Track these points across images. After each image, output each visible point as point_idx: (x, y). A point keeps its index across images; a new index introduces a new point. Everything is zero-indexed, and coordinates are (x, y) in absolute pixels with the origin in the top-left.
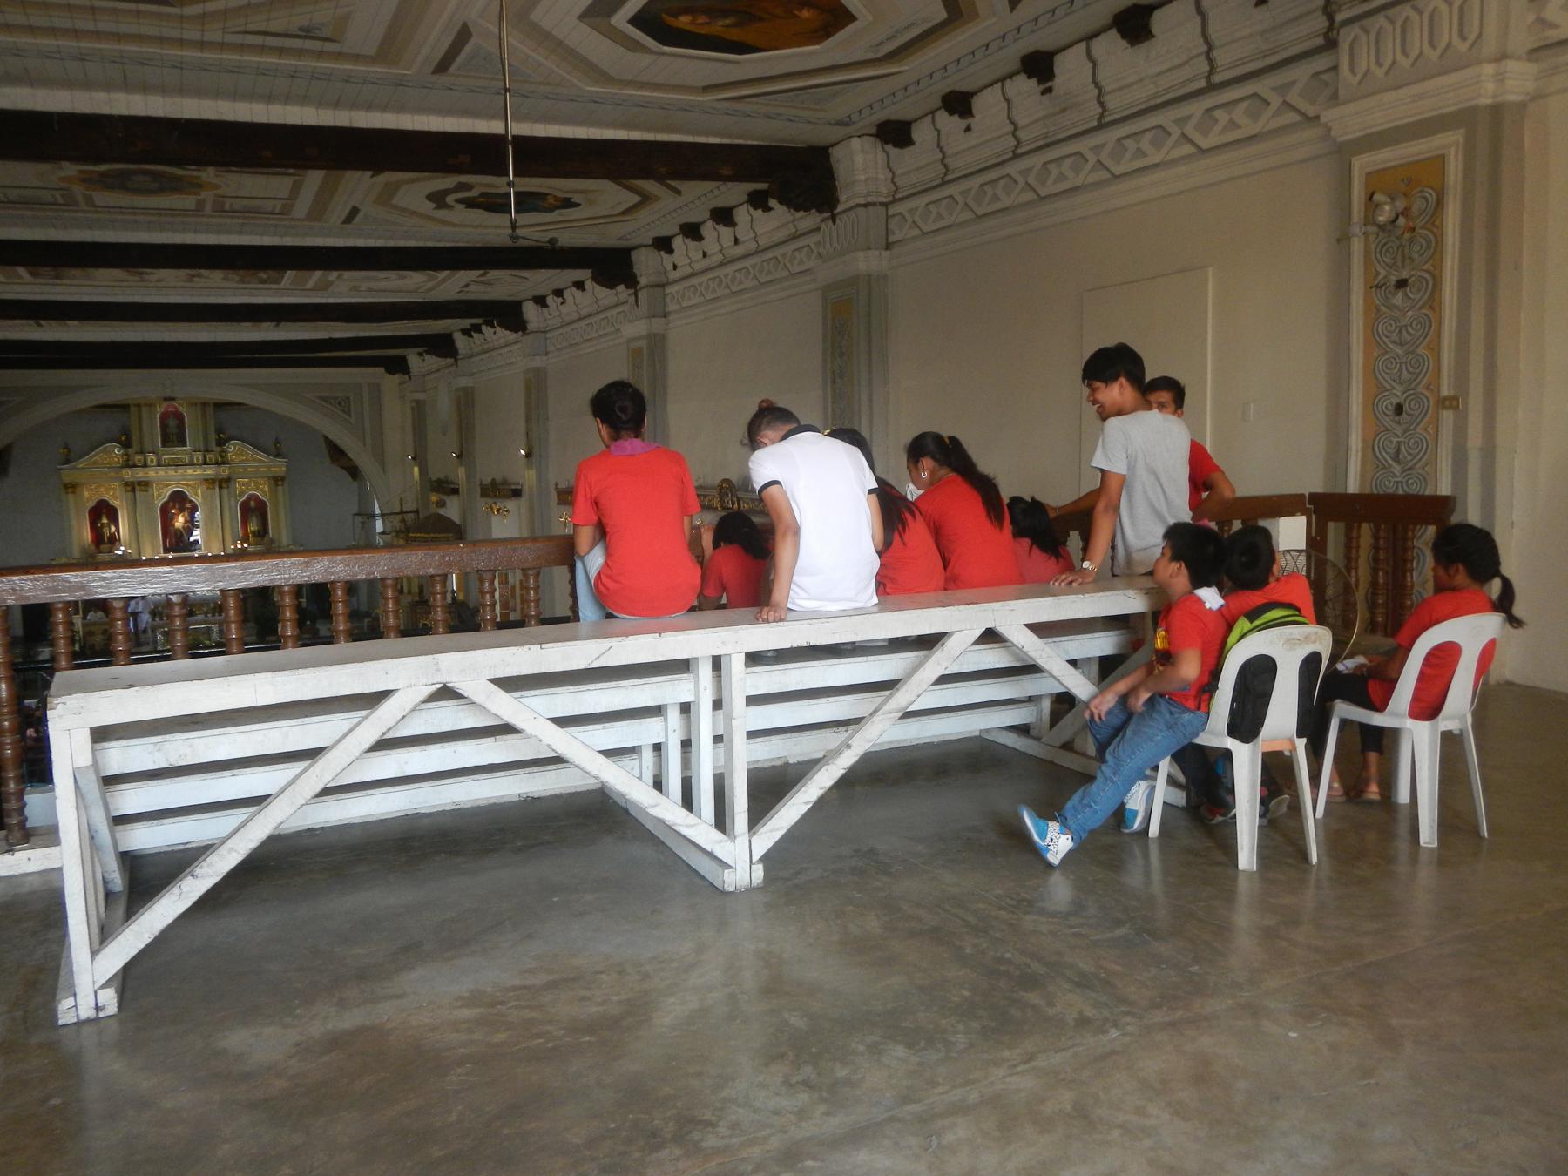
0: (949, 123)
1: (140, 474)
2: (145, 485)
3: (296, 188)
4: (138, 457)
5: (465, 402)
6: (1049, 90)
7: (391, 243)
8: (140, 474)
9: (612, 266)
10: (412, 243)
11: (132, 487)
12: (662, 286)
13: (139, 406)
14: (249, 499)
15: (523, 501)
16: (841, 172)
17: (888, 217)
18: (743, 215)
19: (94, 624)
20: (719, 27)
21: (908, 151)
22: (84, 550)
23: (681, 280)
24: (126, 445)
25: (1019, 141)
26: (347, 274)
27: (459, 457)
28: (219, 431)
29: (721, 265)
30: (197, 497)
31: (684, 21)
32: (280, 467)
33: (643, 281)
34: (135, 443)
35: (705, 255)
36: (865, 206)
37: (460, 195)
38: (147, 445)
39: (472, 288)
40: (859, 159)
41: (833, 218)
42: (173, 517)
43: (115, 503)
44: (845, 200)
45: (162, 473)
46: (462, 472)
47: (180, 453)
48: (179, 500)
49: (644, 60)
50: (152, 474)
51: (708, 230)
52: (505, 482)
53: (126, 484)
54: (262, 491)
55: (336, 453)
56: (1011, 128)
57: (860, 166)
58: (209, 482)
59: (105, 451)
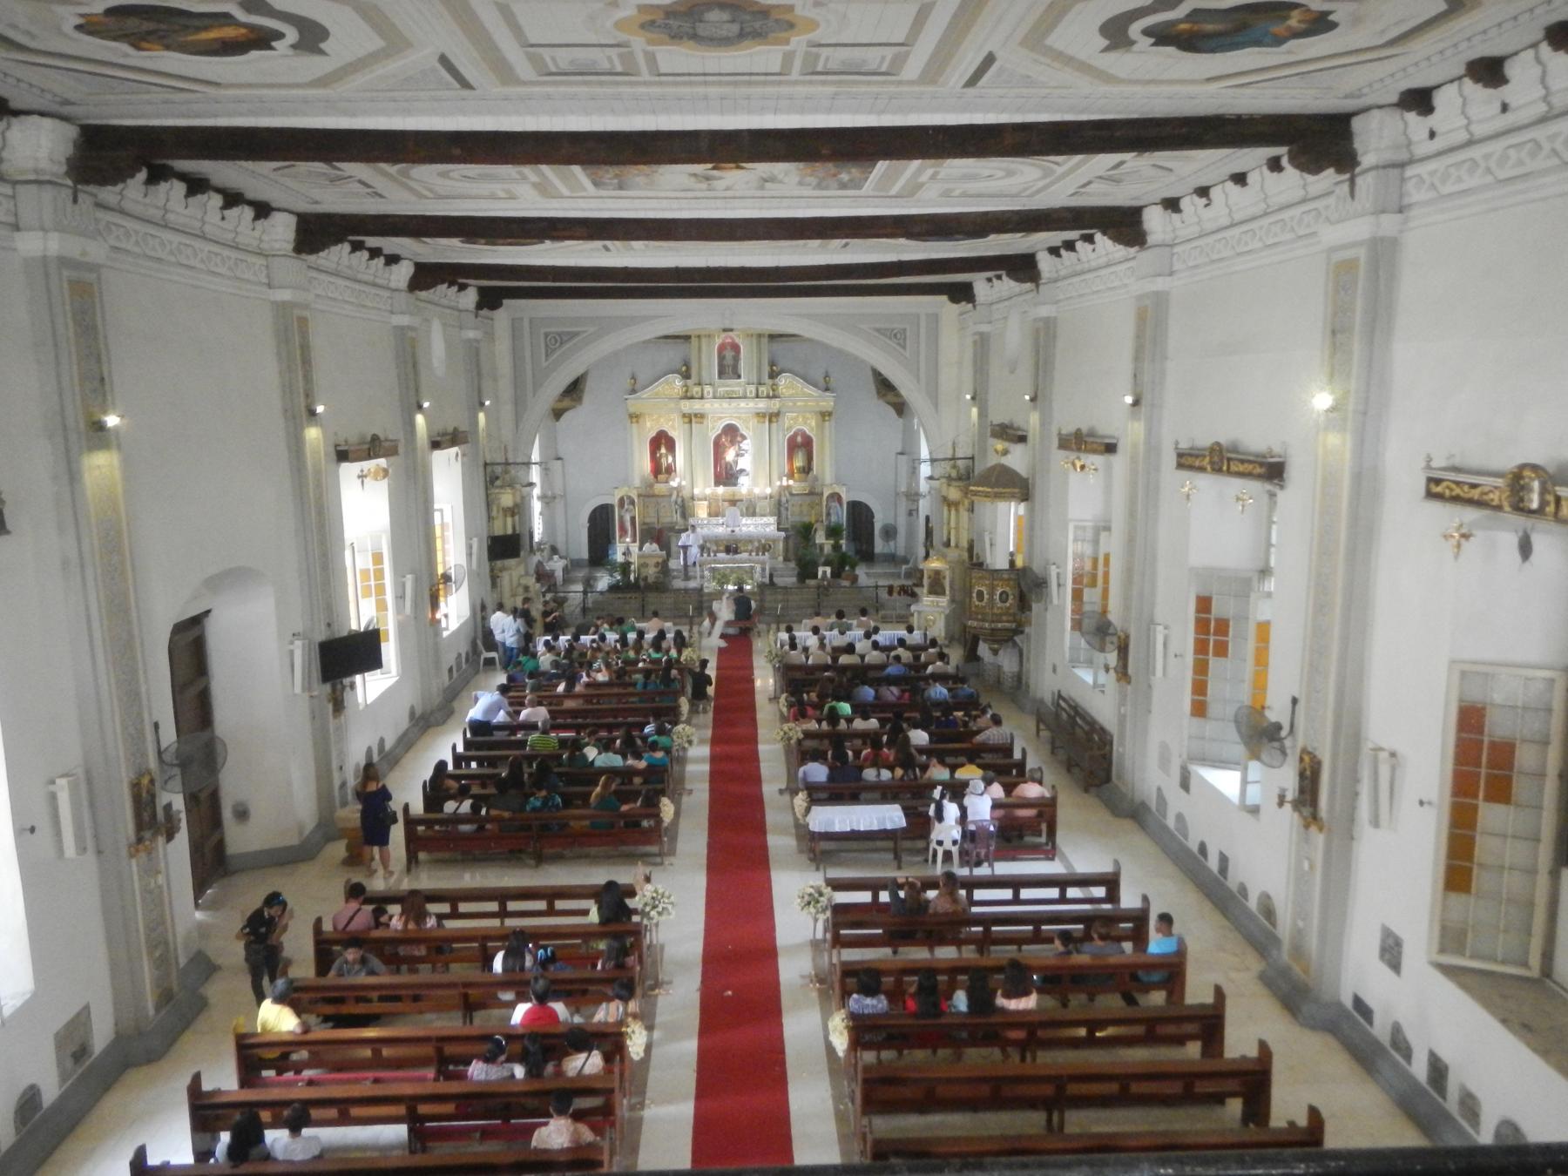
2: (700, 416)
4: (696, 390)
5: (1044, 337)
7: (1018, 118)
11: (689, 418)
12: (1402, 165)
14: (796, 434)
15: (1118, 461)
19: (650, 556)
22: (643, 479)
23: (1440, 154)
27: (1033, 400)
28: (772, 364)
32: (827, 402)
33: (1367, 160)
34: (694, 372)
43: (673, 434)
47: (734, 385)
52: (1092, 434)
53: (684, 416)
54: (809, 426)
58: (760, 415)
59: (667, 382)
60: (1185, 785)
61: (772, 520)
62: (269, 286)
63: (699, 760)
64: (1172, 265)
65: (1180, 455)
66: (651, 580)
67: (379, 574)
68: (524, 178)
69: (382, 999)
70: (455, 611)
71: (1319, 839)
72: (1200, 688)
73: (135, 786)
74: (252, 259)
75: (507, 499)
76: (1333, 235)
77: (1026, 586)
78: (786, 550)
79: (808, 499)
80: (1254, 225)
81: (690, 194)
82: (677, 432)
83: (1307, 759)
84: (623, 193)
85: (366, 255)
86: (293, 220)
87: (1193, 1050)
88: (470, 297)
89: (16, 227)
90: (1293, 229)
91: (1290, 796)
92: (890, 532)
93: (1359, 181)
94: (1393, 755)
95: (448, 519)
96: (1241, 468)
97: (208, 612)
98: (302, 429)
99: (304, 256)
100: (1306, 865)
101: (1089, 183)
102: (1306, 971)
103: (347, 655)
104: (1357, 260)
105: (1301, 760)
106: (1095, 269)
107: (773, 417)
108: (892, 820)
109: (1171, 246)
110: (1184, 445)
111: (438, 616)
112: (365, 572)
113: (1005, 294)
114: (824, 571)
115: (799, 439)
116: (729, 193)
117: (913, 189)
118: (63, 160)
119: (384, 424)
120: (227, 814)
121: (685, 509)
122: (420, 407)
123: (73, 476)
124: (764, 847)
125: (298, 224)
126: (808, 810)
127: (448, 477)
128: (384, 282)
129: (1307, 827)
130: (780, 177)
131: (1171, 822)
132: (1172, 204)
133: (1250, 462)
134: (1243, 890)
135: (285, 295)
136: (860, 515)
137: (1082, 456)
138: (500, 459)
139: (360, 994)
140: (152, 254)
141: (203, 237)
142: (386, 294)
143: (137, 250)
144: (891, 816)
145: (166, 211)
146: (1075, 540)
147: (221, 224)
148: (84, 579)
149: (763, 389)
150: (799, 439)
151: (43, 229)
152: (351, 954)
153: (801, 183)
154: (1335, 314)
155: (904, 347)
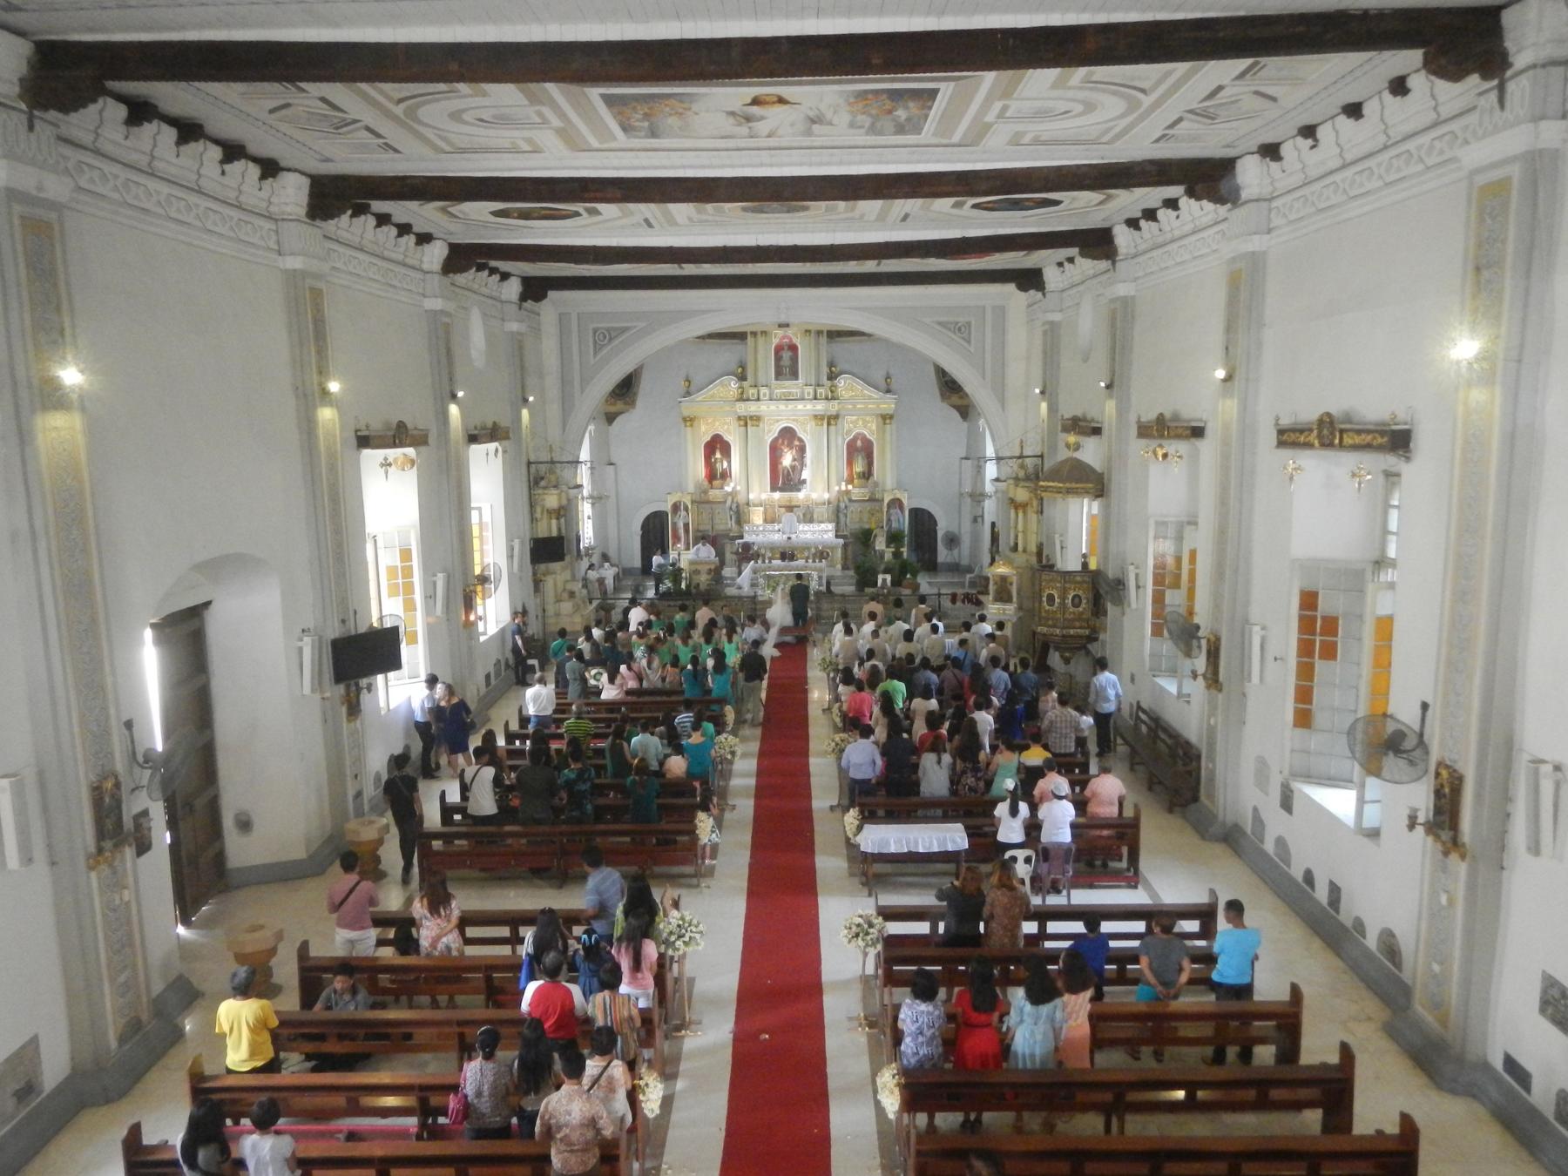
1: (752, 408)
2: (757, 419)
4: (752, 392)
5: (1120, 322)
7: (1102, 18)
8: (752, 408)
11: (745, 421)
13: (754, 334)
14: (854, 440)
22: (698, 486)
24: (742, 378)
27: (1108, 387)
28: (831, 365)
30: (806, 433)
32: (888, 404)
33: (1520, 60)
38: (762, 380)
43: (727, 438)
45: (773, 407)
46: (1110, 407)
47: (791, 387)
48: (788, 434)
50: (764, 408)
52: (1176, 417)
53: (739, 418)
54: (870, 429)
58: (818, 418)
60: (1287, 803)
61: (831, 526)
63: (745, 775)
64: (1269, 220)
65: (1281, 432)
66: (702, 587)
67: (407, 572)
68: (545, 121)
69: (367, 1037)
70: (494, 614)
71: (1461, 868)
72: (1304, 695)
73: (97, 792)
75: (552, 500)
76: (1478, 154)
77: (1101, 590)
78: (845, 558)
79: (868, 506)
80: (1371, 163)
81: (731, 143)
82: (732, 437)
83: (1444, 773)
84: (654, 142)
85: (394, 231)
86: (305, 182)
87: (1312, 1119)
90: (1421, 160)
91: (1421, 819)
92: (952, 541)
93: (1511, 87)
94: (1557, 768)
95: (487, 518)
96: (1358, 440)
97: (207, 604)
98: (315, 407)
99: (318, 223)
100: (1444, 899)
101: (1180, 120)
102: (1444, 1022)
103: (363, 654)
104: (1508, 179)
105: (1438, 775)
106: (1181, 238)
107: (832, 420)
108: (954, 842)
109: (1270, 200)
110: (1285, 422)
111: (472, 618)
112: (392, 571)
113: (1077, 279)
114: (884, 579)
115: (859, 443)
116: (772, 142)
117: (979, 133)
118: (15, 80)
119: (416, 415)
120: (228, 822)
121: (740, 516)
122: (454, 397)
123: (24, 437)
124: (811, 872)
125: (312, 186)
126: (860, 829)
127: (487, 479)
128: (415, 263)
129: (1446, 854)
130: (829, 115)
131: (1269, 846)
132: (1271, 151)
133: (1369, 432)
134: (1359, 926)
136: (923, 522)
137: (1164, 442)
138: (545, 457)
139: (347, 1029)
140: (136, 203)
141: (200, 192)
142: (419, 275)
143: (116, 196)
144: (953, 837)
145: (153, 157)
146: (1156, 538)
147: (221, 179)
148: (35, 551)
149: (820, 390)
150: (859, 443)
152: (339, 983)
153: (852, 125)
154: (1479, 245)
155: (969, 342)
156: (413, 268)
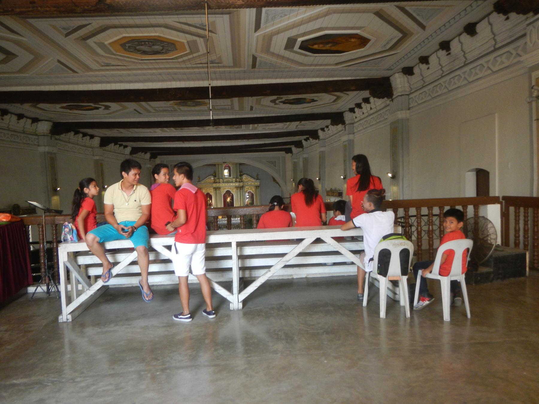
0: (424, 66)
1: (217, 185)
2: (219, 188)
3: (232, 102)
4: (218, 180)
6: (449, 54)
7: (267, 115)
8: (217, 185)
9: (337, 118)
10: (273, 115)
11: (216, 189)
12: (353, 124)
16: (393, 85)
17: (409, 99)
18: (372, 100)
20: (328, 47)
21: (413, 77)
23: (358, 121)
24: (215, 176)
25: (443, 71)
26: (260, 125)
28: (240, 172)
29: (367, 116)
31: (316, 47)
32: (257, 183)
33: (347, 122)
34: (217, 175)
35: (363, 113)
36: (401, 95)
37: (280, 100)
39: (299, 126)
40: (398, 81)
41: (392, 100)
42: (227, 198)
43: (212, 194)
44: (396, 94)
48: (228, 193)
49: (312, 58)
51: (363, 105)
55: (274, 180)
56: (440, 67)
57: (399, 82)
58: (237, 188)
62: (93, 155)
74: (89, 149)
82: (212, 194)
88: (148, 155)
89: (38, 145)
135: (97, 158)
141: (78, 144)
151: (44, 146)
156: (123, 154)
